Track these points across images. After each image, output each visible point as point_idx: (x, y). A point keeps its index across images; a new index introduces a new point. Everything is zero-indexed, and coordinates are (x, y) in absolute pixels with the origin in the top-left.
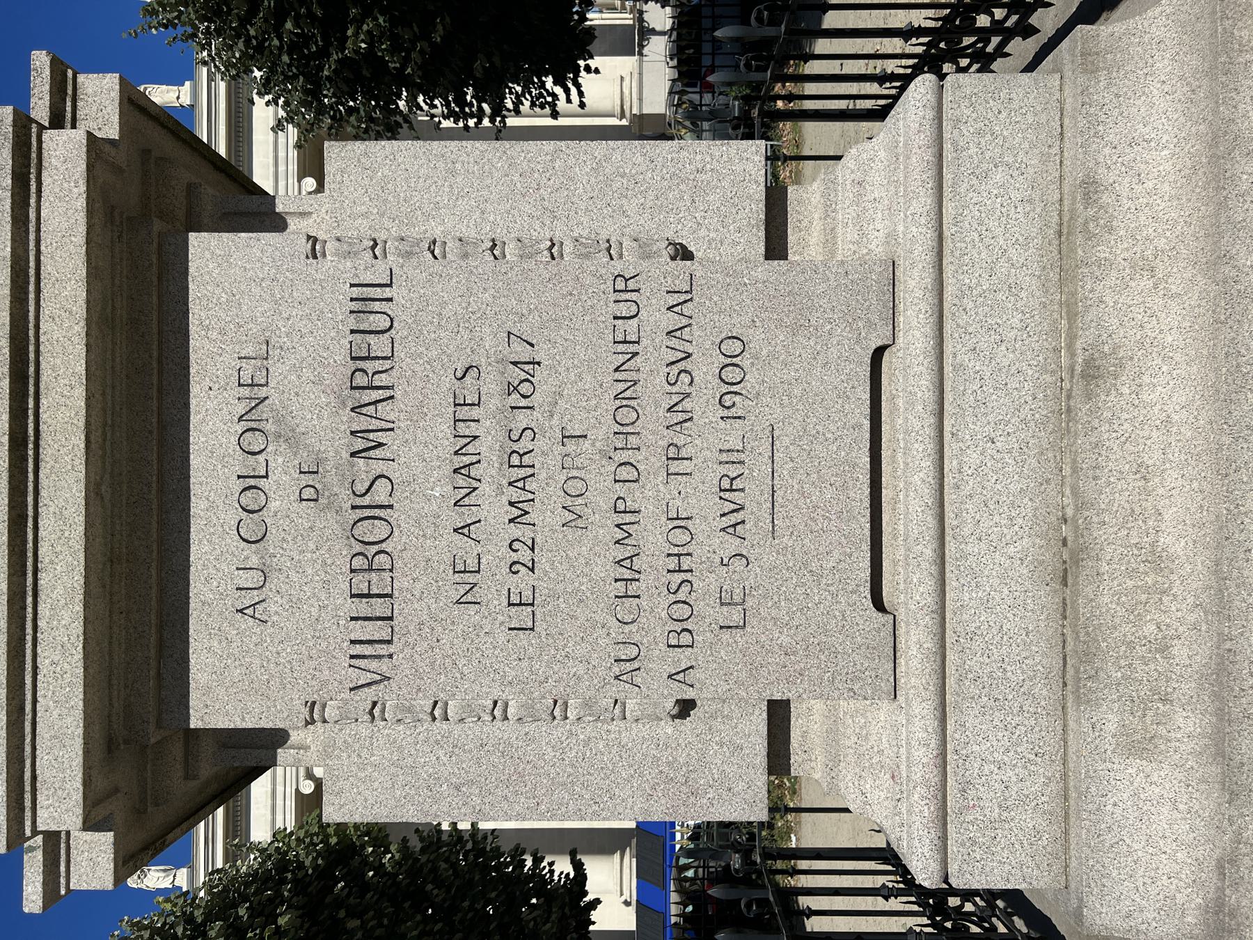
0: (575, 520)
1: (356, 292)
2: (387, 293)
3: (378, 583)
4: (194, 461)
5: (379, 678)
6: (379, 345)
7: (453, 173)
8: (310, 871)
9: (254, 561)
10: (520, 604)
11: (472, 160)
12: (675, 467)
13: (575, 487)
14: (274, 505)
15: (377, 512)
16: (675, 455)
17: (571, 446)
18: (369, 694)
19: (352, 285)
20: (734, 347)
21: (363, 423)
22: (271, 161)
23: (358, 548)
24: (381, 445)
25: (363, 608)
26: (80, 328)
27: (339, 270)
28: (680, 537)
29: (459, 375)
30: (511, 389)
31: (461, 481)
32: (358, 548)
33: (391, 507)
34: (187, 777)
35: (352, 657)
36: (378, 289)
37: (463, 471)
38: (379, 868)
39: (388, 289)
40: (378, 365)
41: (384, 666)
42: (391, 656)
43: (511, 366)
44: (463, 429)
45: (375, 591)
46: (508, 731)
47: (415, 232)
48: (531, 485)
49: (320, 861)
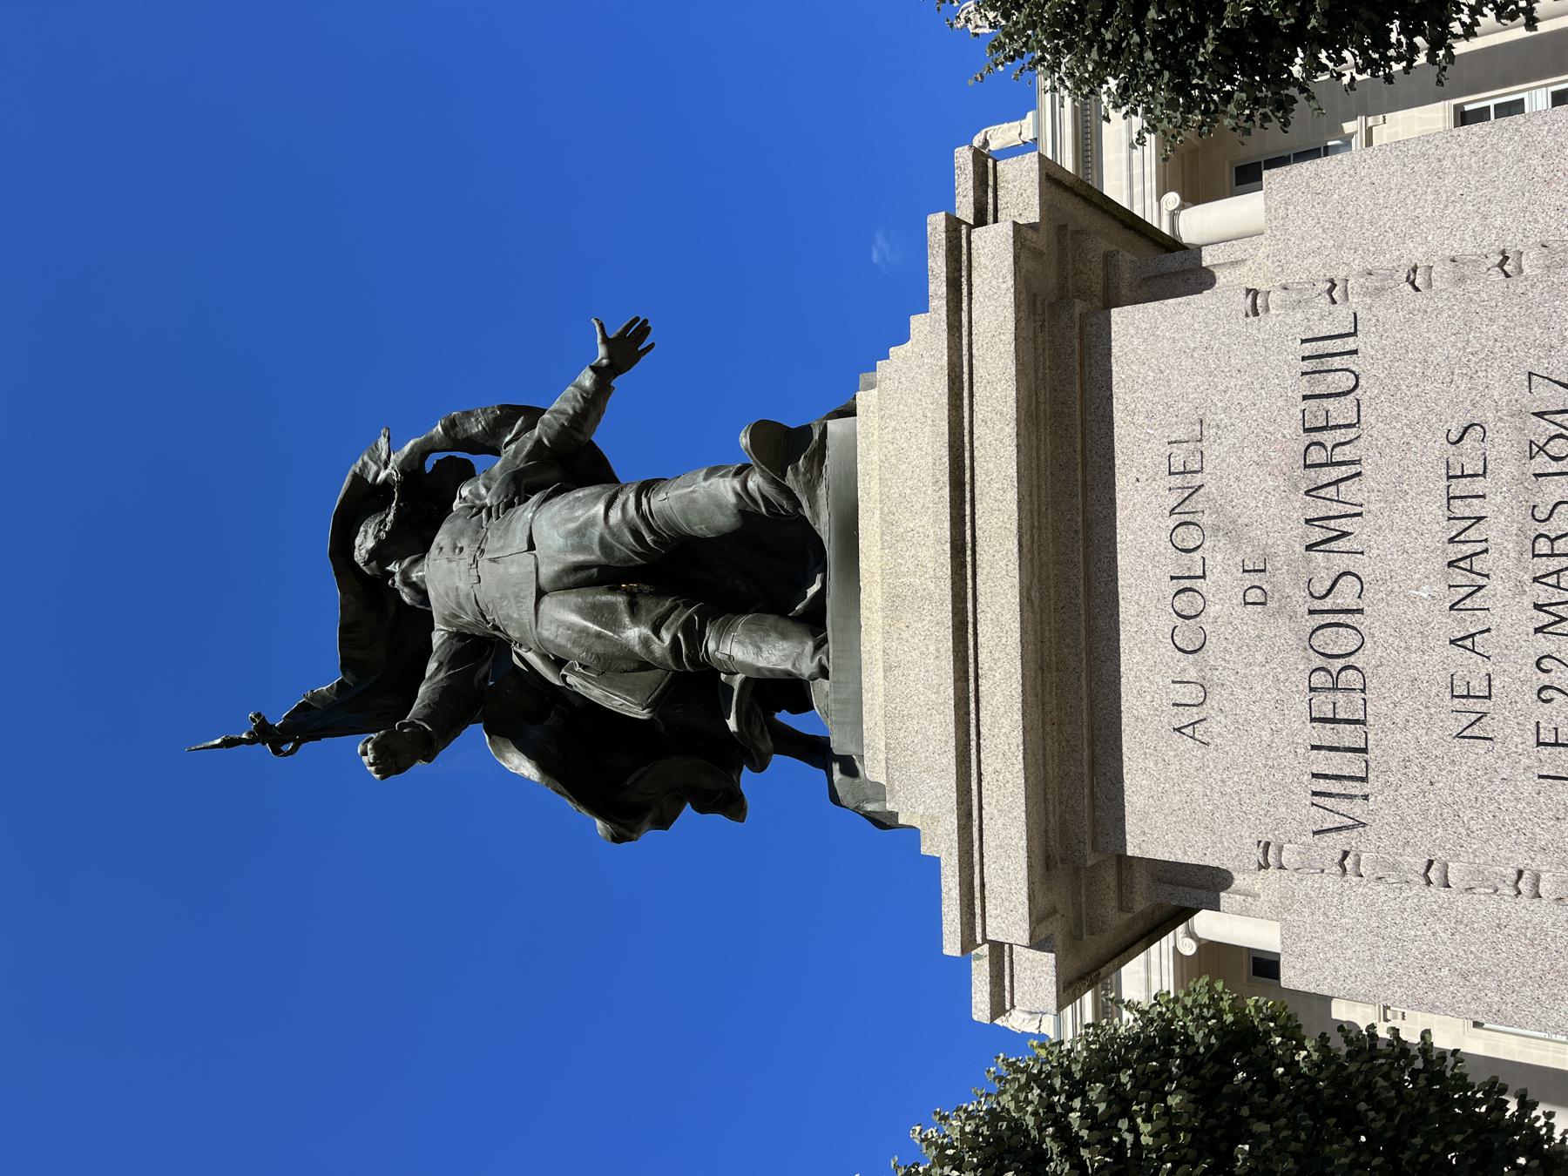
1: (1309, 349)
2: (1350, 344)
3: (1347, 706)
4: (1123, 561)
5: (1351, 822)
6: (1341, 410)
7: (1440, 174)
8: (1202, 1050)
9: (1192, 674)
10: (1556, 744)
11: (1467, 151)
14: (1212, 610)
15: (1342, 618)
18: (1339, 841)
19: (1303, 341)
21: (1321, 508)
22: (1125, 183)
23: (1319, 662)
24: (1344, 534)
25: (1327, 735)
26: (1011, 429)
27: (1286, 328)
29: (1453, 437)
30: (1535, 449)
31: (1458, 577)
32: (1319, 662)
33: (1360, 611)
34: (1121, 909)
35: (1315, 794)
36: (1339, 341)
37: (1461, 564)
38: (1291, 1065)
39: (1351, 339)
40: (1339, 435)
41: (1357, 809)
42: (1366, 797)
43: (1535, 419)
44: (1459, 508)
45: (1341, 715)
46: (1543, 913)
47: (1385, 261)
49: (1213, 1040)
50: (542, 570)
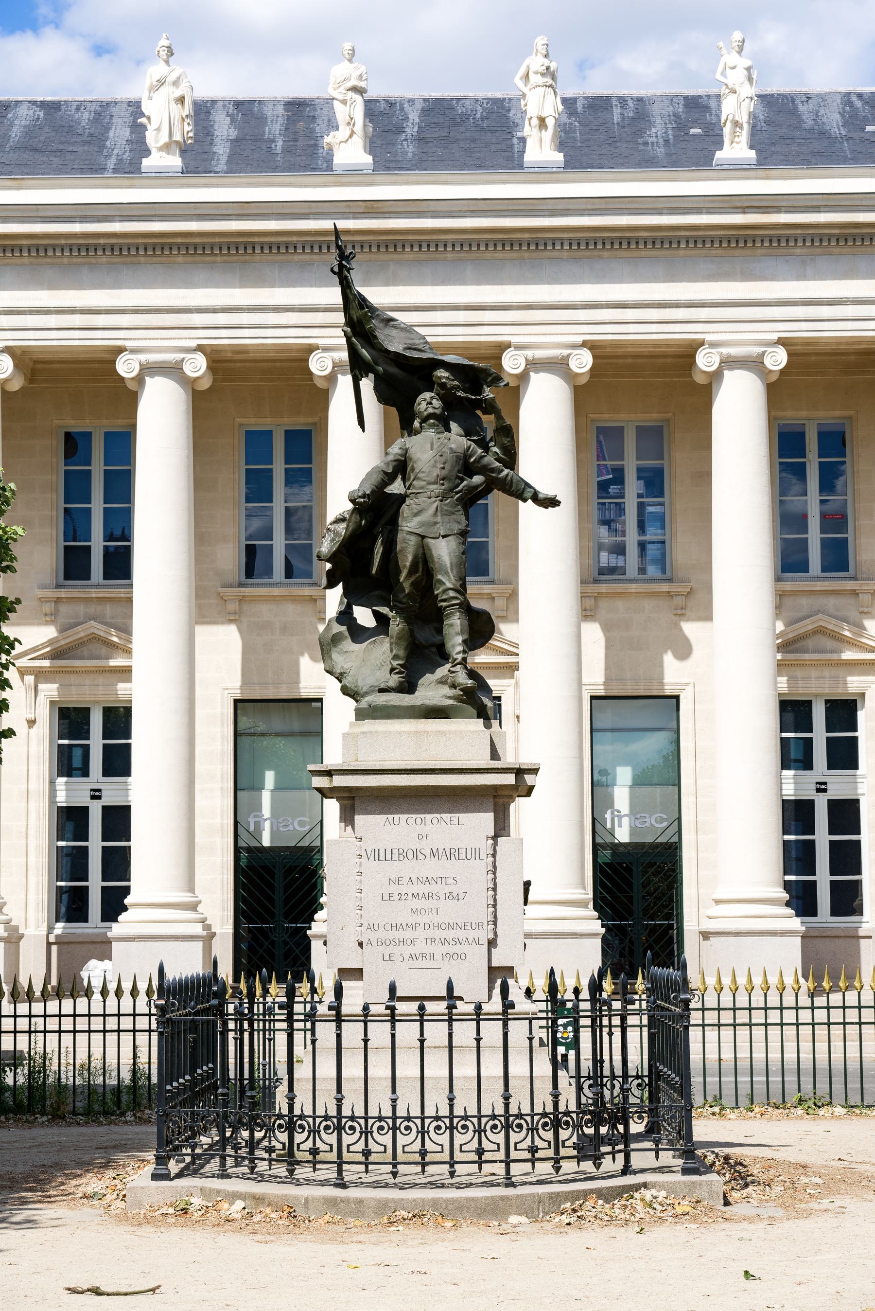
0: (413, 912)
3: (395, 857)
12: (429, 940)
13: (423, 912)
16: (433, 940)
17: (434, 911)
18: (364, 854)
20: (463, 957)
21: (440, 852)
28: (409, 942)
31: (425, 879)
48: (424, 899)
50: (433, 541)
